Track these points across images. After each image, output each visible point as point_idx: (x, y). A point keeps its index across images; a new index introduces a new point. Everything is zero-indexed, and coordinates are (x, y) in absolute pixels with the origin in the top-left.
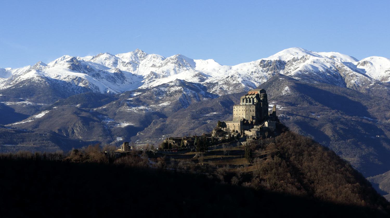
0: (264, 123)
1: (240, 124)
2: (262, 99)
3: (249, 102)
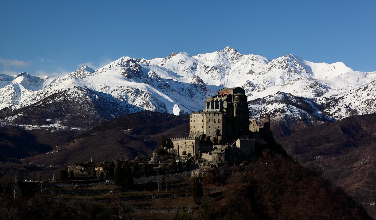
0: (236, 142)
1: (194, 143)
2: (237, 103)
3: (216, 108)
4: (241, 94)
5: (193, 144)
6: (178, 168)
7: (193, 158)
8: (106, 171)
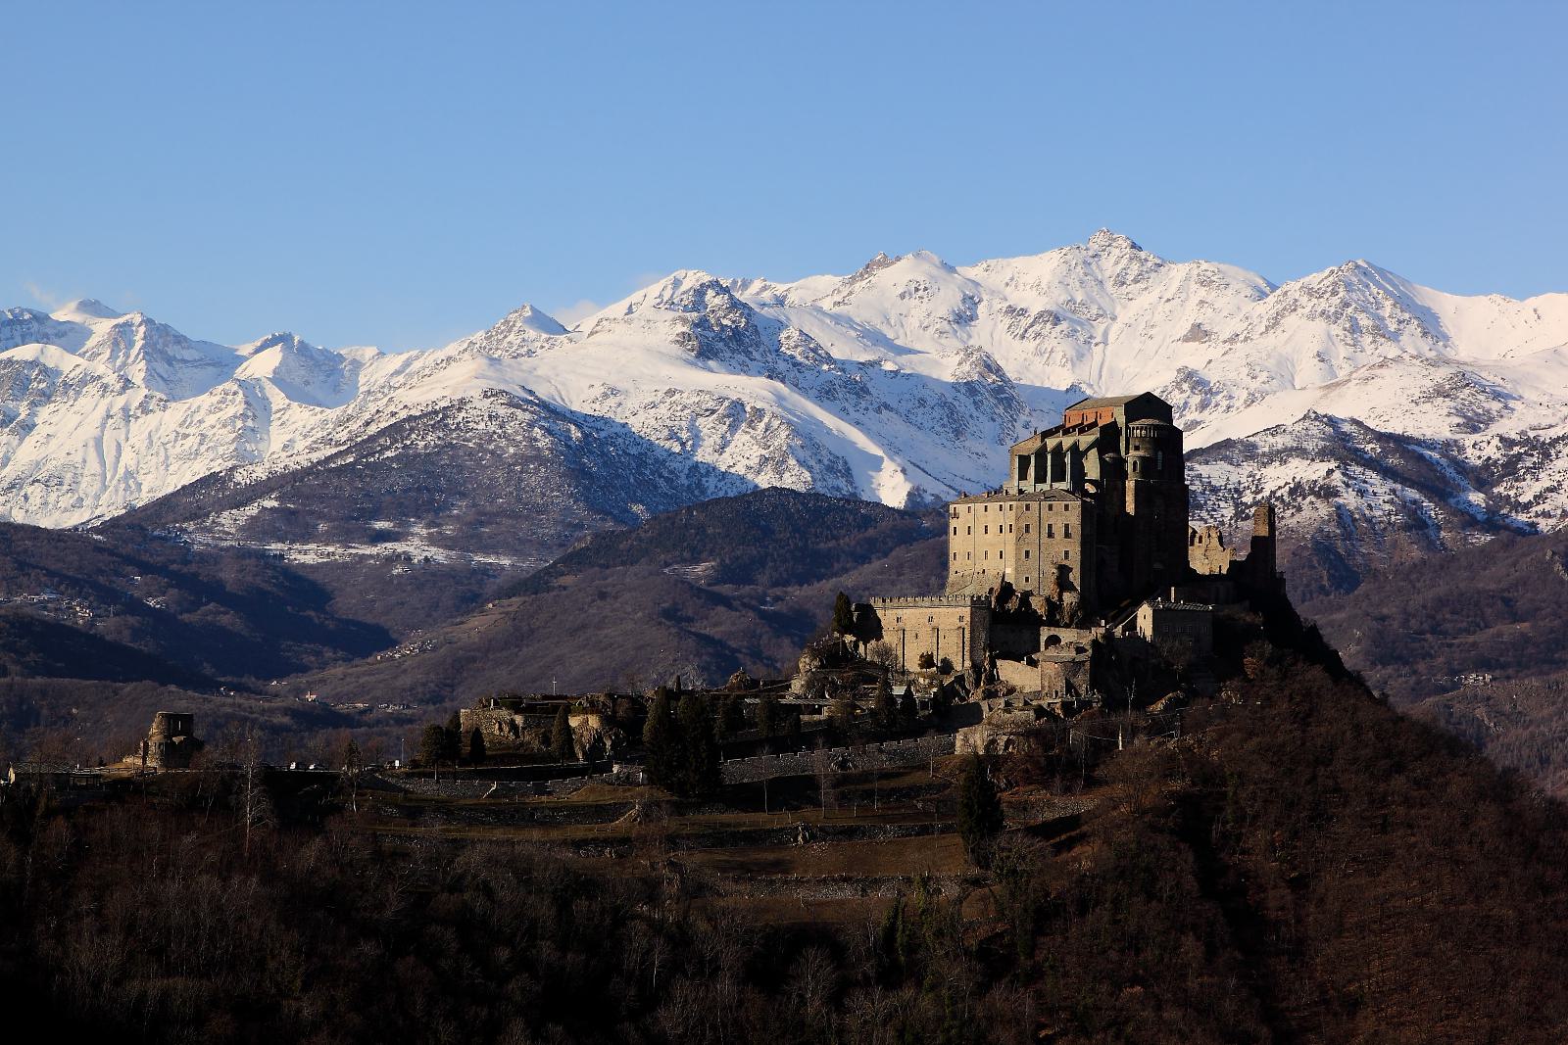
0: (1136, 616)
1: (968, 619)
2: (1140, 457)
4: (1156, 422)
5: (964, 623)
6: (905, 719)
7: (960, 679)
8: (611, 729)
